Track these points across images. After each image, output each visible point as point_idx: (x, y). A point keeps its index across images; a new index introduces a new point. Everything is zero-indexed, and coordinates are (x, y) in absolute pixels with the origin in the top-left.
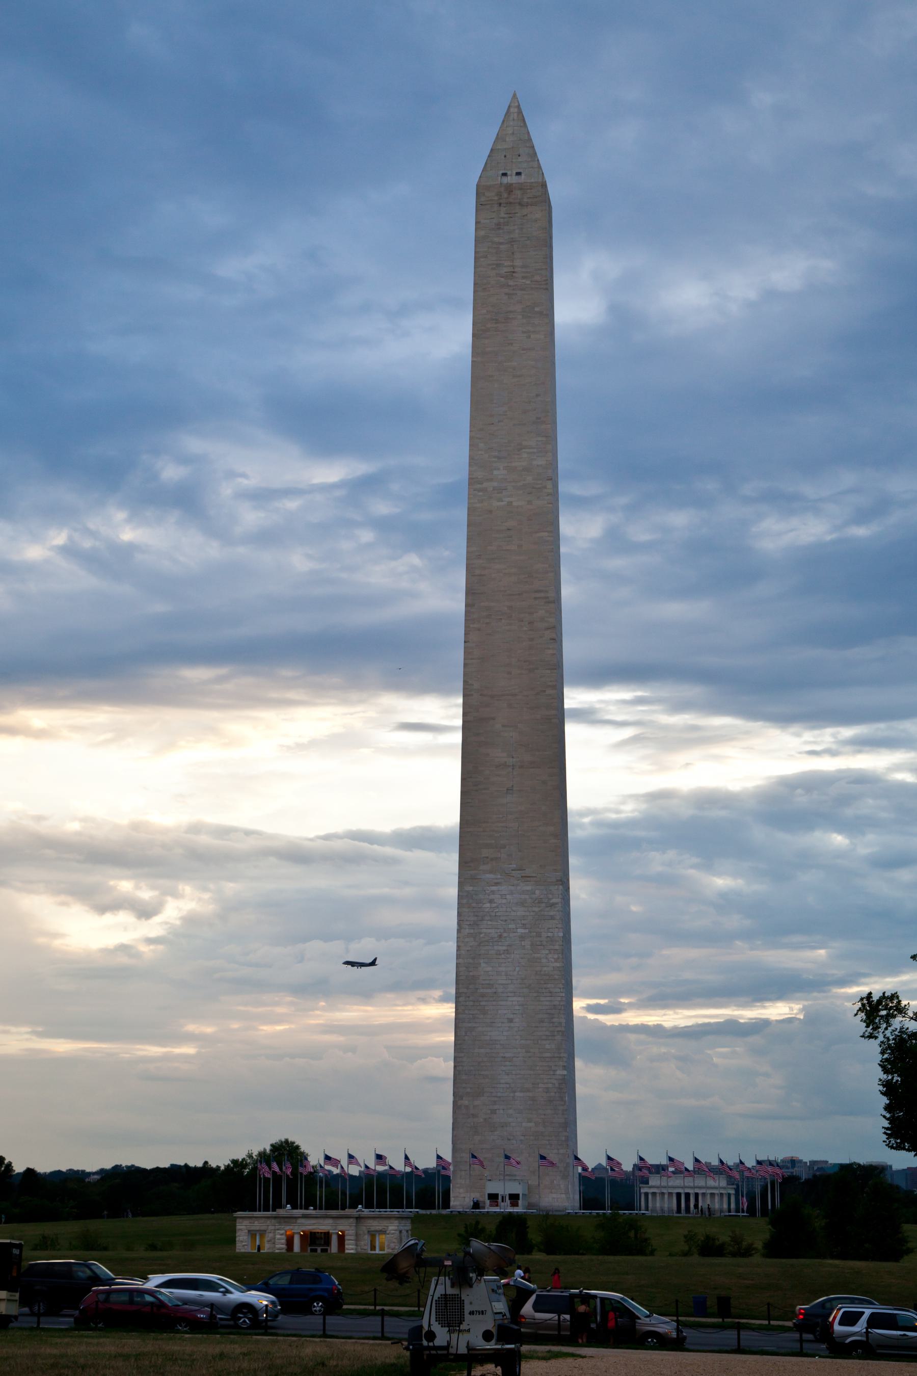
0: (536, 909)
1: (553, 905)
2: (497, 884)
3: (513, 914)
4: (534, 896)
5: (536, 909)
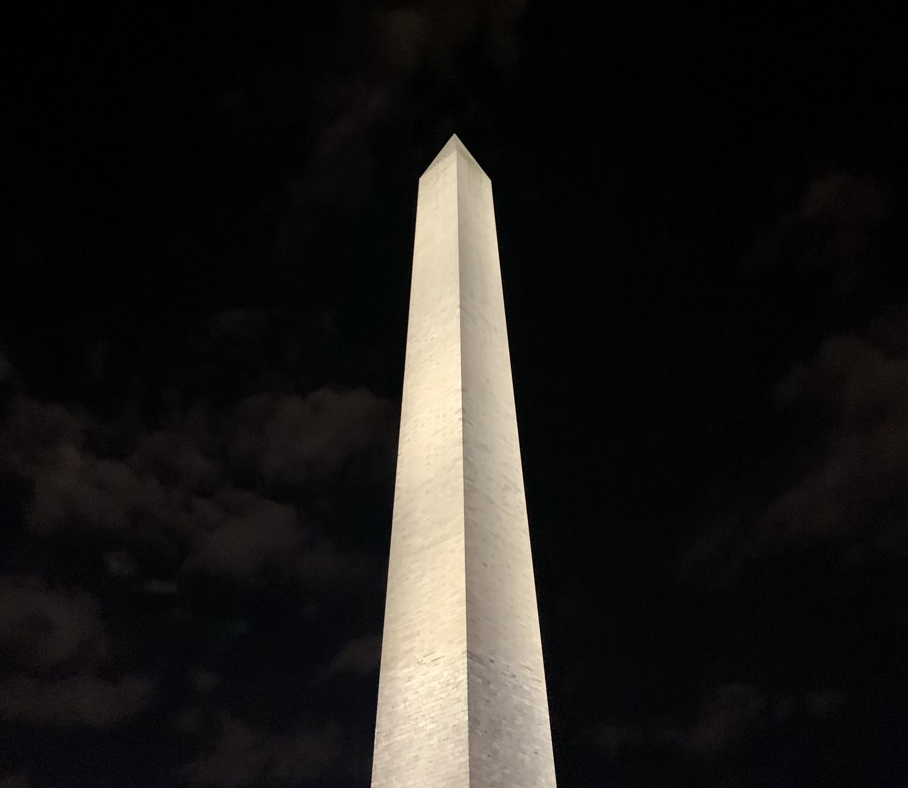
0: (443, 695)
1: (458, 685)
2: (410, 679)
3: (424, 708)
4: (442, 680)
5: (443, 695)
